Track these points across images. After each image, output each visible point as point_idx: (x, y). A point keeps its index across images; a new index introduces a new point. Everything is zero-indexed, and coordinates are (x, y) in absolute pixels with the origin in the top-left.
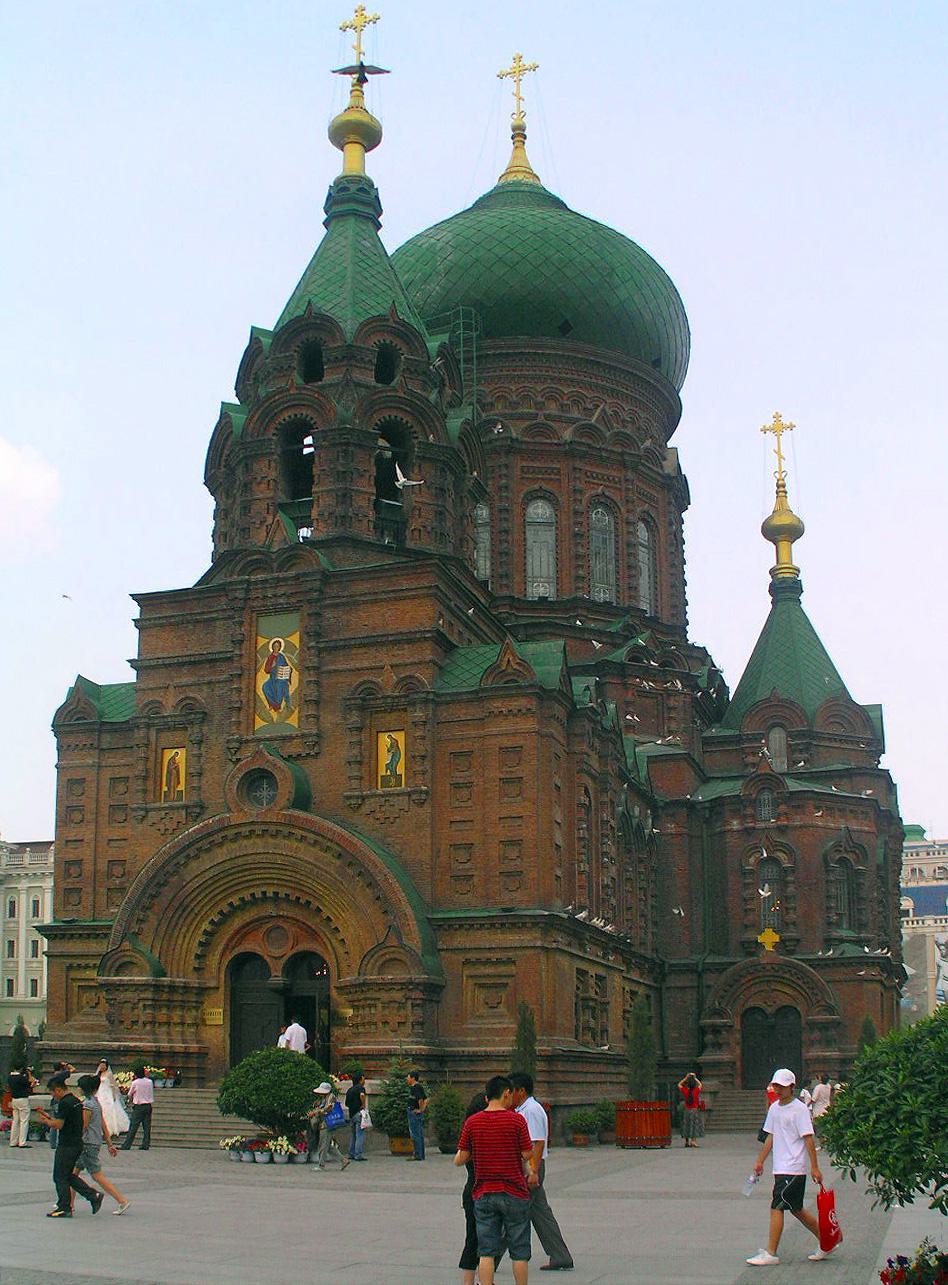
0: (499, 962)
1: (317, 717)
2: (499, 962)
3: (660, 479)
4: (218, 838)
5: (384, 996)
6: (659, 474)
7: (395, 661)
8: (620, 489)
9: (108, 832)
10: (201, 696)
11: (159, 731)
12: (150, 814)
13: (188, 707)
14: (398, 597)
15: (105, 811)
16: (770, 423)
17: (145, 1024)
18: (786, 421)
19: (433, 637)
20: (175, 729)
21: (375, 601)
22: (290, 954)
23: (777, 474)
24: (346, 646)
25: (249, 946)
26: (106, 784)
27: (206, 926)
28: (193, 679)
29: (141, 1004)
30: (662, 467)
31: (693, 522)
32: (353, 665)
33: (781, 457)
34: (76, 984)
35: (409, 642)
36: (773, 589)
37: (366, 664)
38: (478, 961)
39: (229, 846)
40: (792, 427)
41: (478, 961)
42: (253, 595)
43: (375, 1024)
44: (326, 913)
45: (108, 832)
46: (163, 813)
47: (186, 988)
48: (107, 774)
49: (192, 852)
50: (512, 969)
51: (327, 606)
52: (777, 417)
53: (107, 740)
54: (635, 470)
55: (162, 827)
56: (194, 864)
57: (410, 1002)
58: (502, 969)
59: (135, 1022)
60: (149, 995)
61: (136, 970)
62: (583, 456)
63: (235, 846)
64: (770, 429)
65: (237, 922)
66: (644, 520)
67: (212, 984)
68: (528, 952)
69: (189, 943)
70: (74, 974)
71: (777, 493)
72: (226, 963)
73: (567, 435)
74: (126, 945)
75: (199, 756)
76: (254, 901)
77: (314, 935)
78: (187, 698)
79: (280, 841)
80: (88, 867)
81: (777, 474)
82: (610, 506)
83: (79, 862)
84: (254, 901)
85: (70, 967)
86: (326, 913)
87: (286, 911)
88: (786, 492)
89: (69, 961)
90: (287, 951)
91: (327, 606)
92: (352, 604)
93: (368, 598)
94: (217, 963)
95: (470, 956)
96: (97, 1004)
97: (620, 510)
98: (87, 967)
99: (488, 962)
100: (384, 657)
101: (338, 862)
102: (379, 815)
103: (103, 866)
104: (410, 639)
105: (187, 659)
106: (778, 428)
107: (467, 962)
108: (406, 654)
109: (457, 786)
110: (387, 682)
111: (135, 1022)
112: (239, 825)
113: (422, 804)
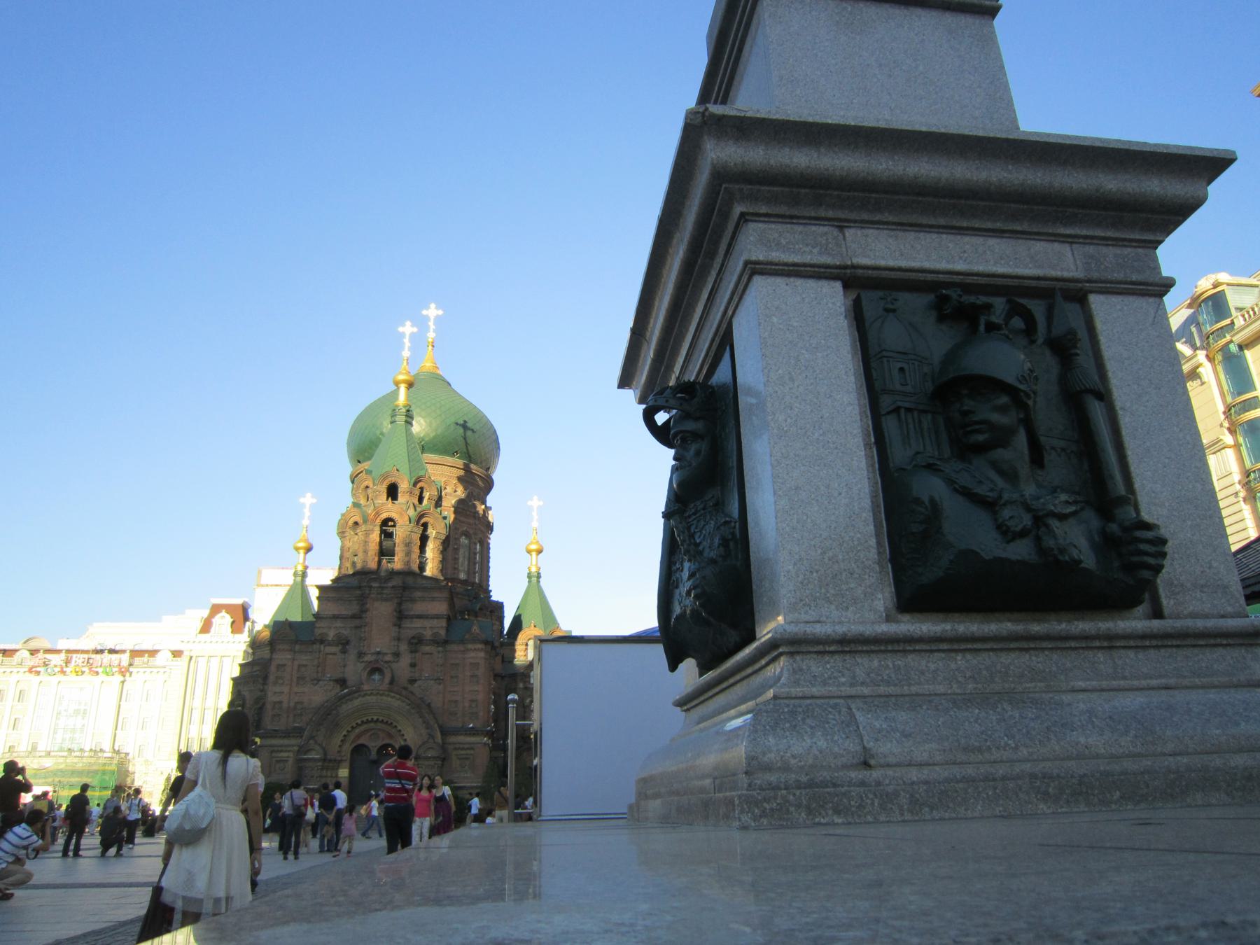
0: (468, 749)
1: (398, 646)
2: (468, 749)
4: (356, 695)
5: (426, 763)
7: (431, 625)
9: (295, 689)
11: (325, 646)
12: (321, 683)
14: (433, 599)
15: (295, 680)
17: (317, 777)
20: (332, 645)
21: (424, 600)
22: (380, 745)
24: (412, 617)
25: (360, 742)
26: (296, 667)
27: (345, 733)
28: (342, 625)
29: (316, 768)
31: (495, 540)
34: (275, 759)
35: (437, 618)
37: (419, 626)
38: (459, 749)
39: (360, 699)
41: (459, 749)
42: (372, 592)
44: (399, 728)
45: (295, 689)
46: (326, 682)
47: (335, 760)
48: (296, 663)
49: (344, 701)
50: (472, 752)
53: (297, 647)
56: (344, 706)
57: (436, 766)
58: (469, 752)
59: (312, 777)
60: (320, 764)
61: (314, 752)
65: (357, 731)
66: (480, 542)
67: (344, 758)
68: (479, 745)
69: (337, 740)
70: (274, 754)
72: (351, 749)
74: (311, 742)
75: (344, 659)
76: (368, 722)
77: (390, 736)
79: (385, 698)
80: (285, 705)
83: (280, 702)
84: (368, 722)
85: (272, 752)
86: (399, 728)
87: (379, 725)
89: (272, 749)
90: (380, 743)
92: (413, 601)
94: (348, 748)
95: (457, 746)
96: (284, 769)
98: (281, 751)
99: (463, 749)
100: (427, 623)
101: (408, 707)
102: (422, 688)
103: (292, 704)
104: (437, 617)
107: (455, 749)
108: (435, 623)
109: (452, 677)
110: (428, 634)
111: (312, 777)
112: (366, 691)
113: (440, 684)
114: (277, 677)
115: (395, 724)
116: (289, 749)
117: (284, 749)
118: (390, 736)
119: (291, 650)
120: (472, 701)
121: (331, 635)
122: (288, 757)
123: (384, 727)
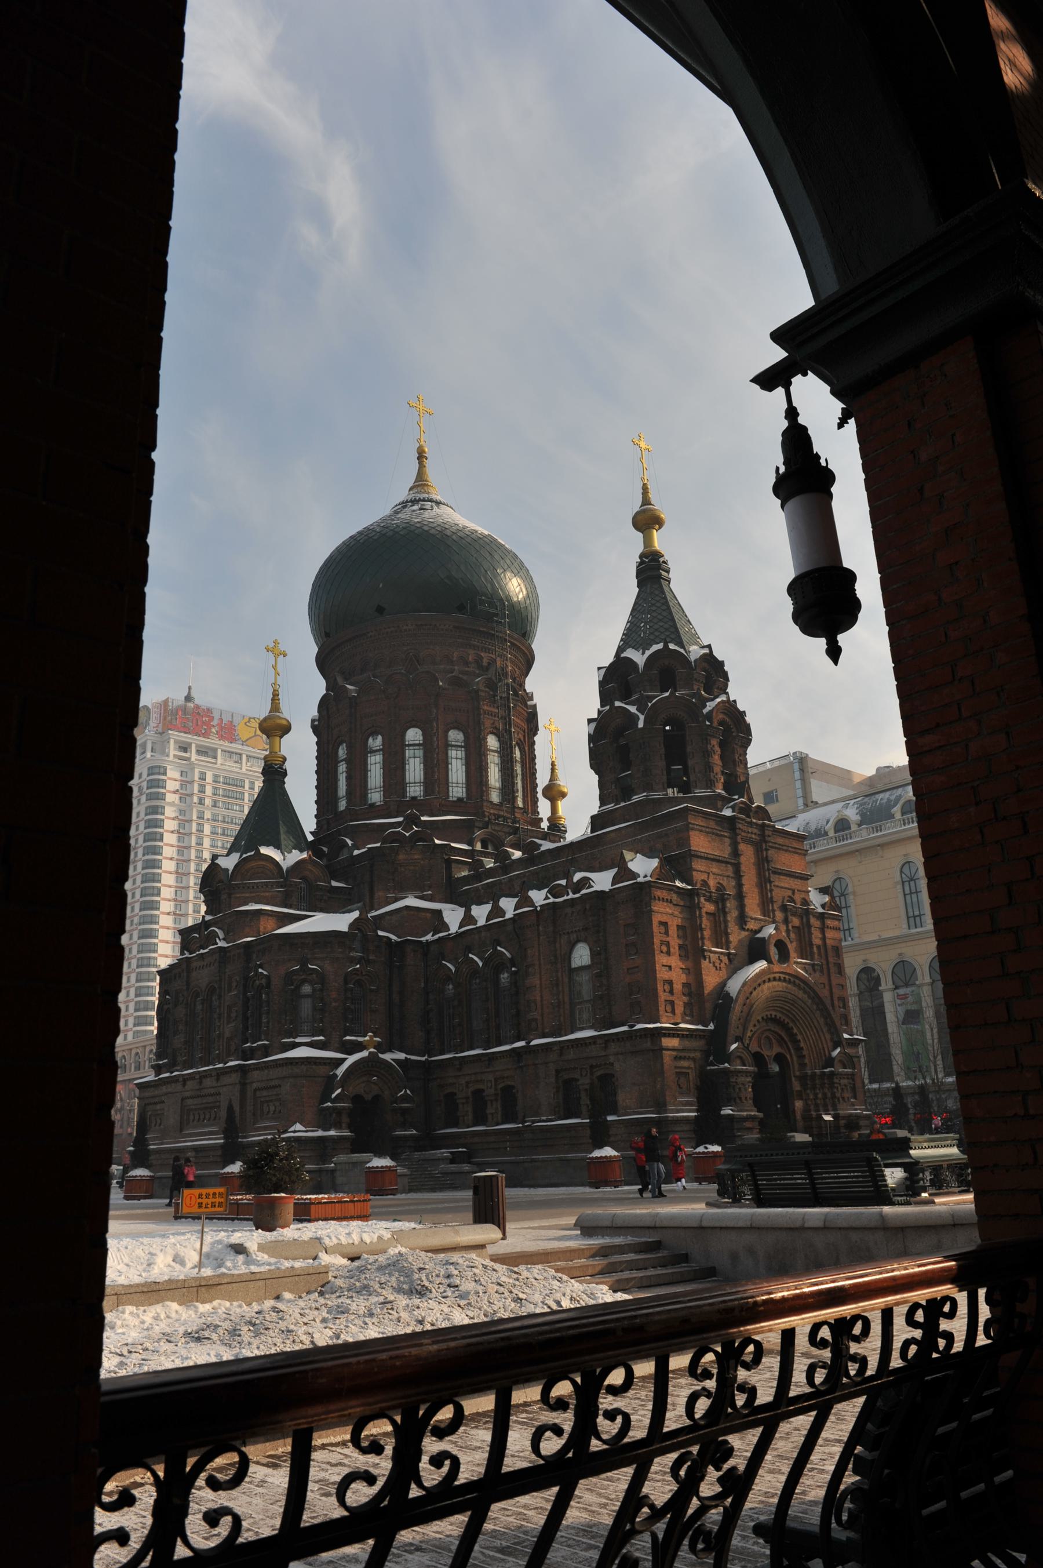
10: (725, 883)
13: (720, 888)
15: (677, 948)
21: (786, 851)
32: (782, 885)
37: (787, 886)
43: (839, 1099)
46: (717, 955)
51: (772, 847)
55: (717, 965)
63: (770, 984)
78: (719, 883)
91: (772, 847)
92: (780, 848)
93: (785, 848)
98: (684, 1058)
101: (810, 1001)
105: (718, 858)
112: (776, 973)
114: (662, 943)
115: (791, 1025)
116: (692, 1055)
117: (687, 1055)
118: (781, 1041)
119: (671, 902)
120: (839, 999)
121: (712, 883)
122: (688, 1068)
123: (777, 1029)
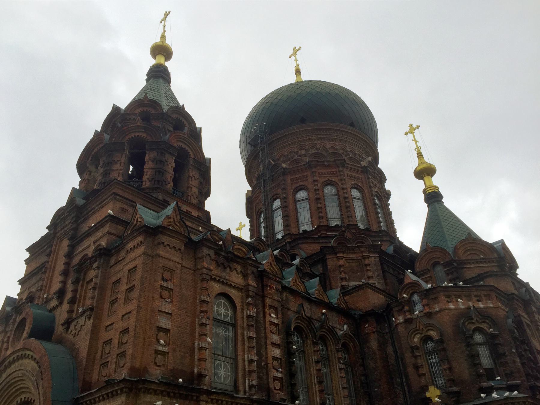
3: (360, 169)
6: (359, 167)
8: (337, 176)
16: (408, 129)
18: (414, 126)
19: (109, 219)
23: (416, 150)
30: (360, 164)
33: (416, 142)
36: (426, 200)
40: (418, 127)
52: (411, 126)
54: (343, 166)
62: (316, 166)
64: (409, 132)
71: (418, 157)
73: (307, 159)
81: (416, 150)
82: (330, 183)
88: (423, 156)
97: (338, 184)
106: (412, 130)
